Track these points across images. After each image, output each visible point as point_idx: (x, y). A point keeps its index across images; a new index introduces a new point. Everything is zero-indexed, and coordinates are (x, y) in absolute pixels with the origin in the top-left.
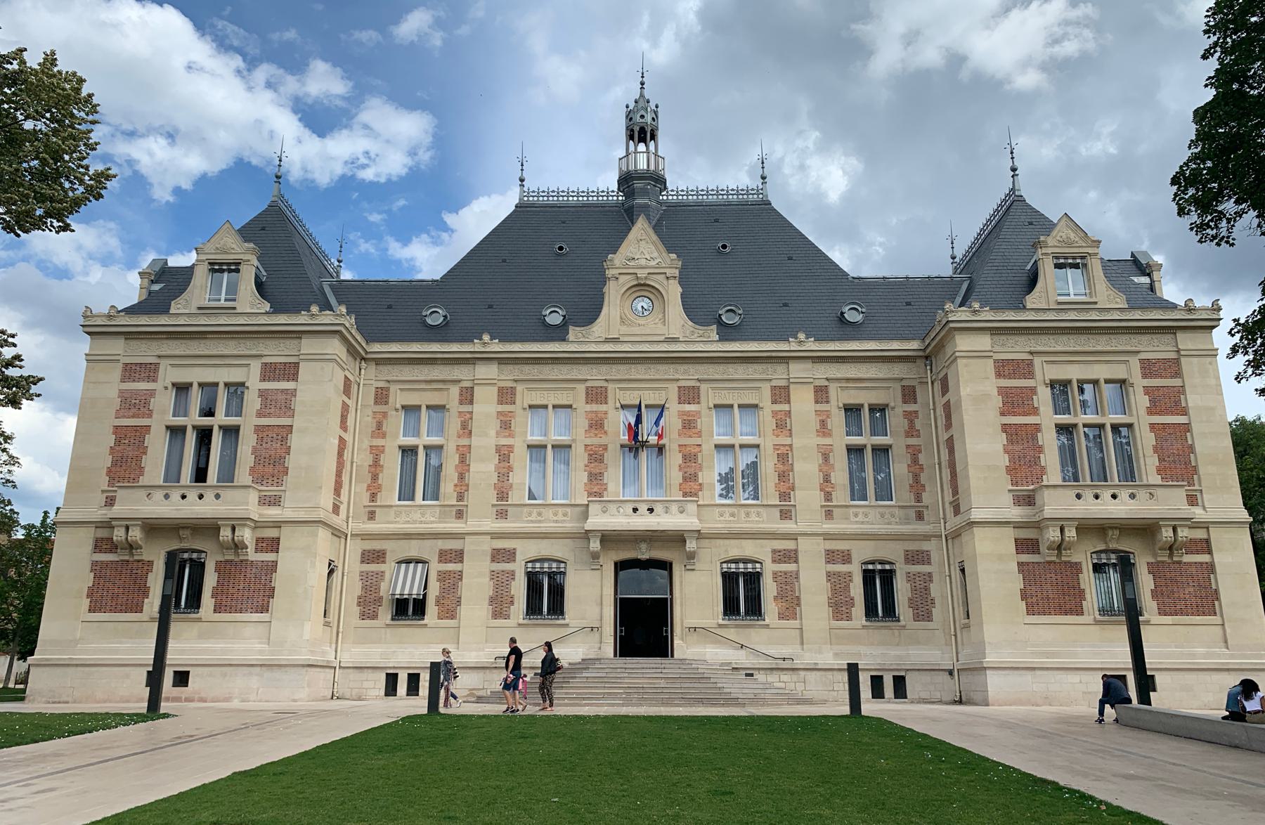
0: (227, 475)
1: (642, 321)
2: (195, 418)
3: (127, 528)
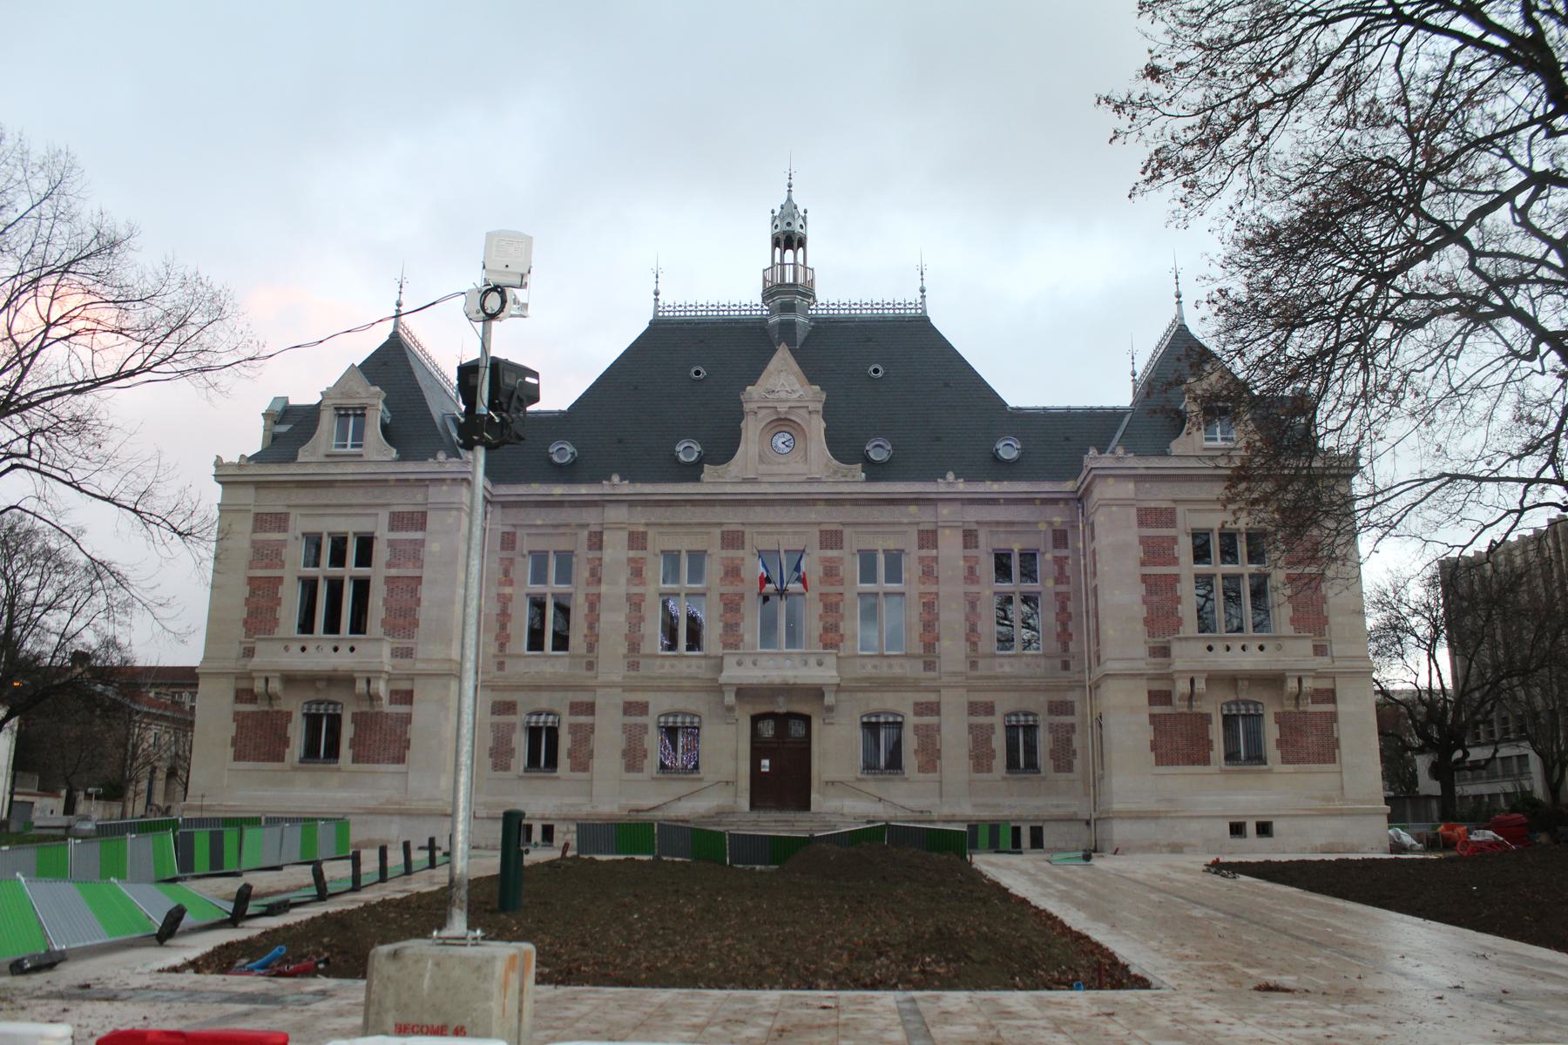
0: (358, 626)
1: (782, 459)
2: (325, 569)
3: (267, 680)
